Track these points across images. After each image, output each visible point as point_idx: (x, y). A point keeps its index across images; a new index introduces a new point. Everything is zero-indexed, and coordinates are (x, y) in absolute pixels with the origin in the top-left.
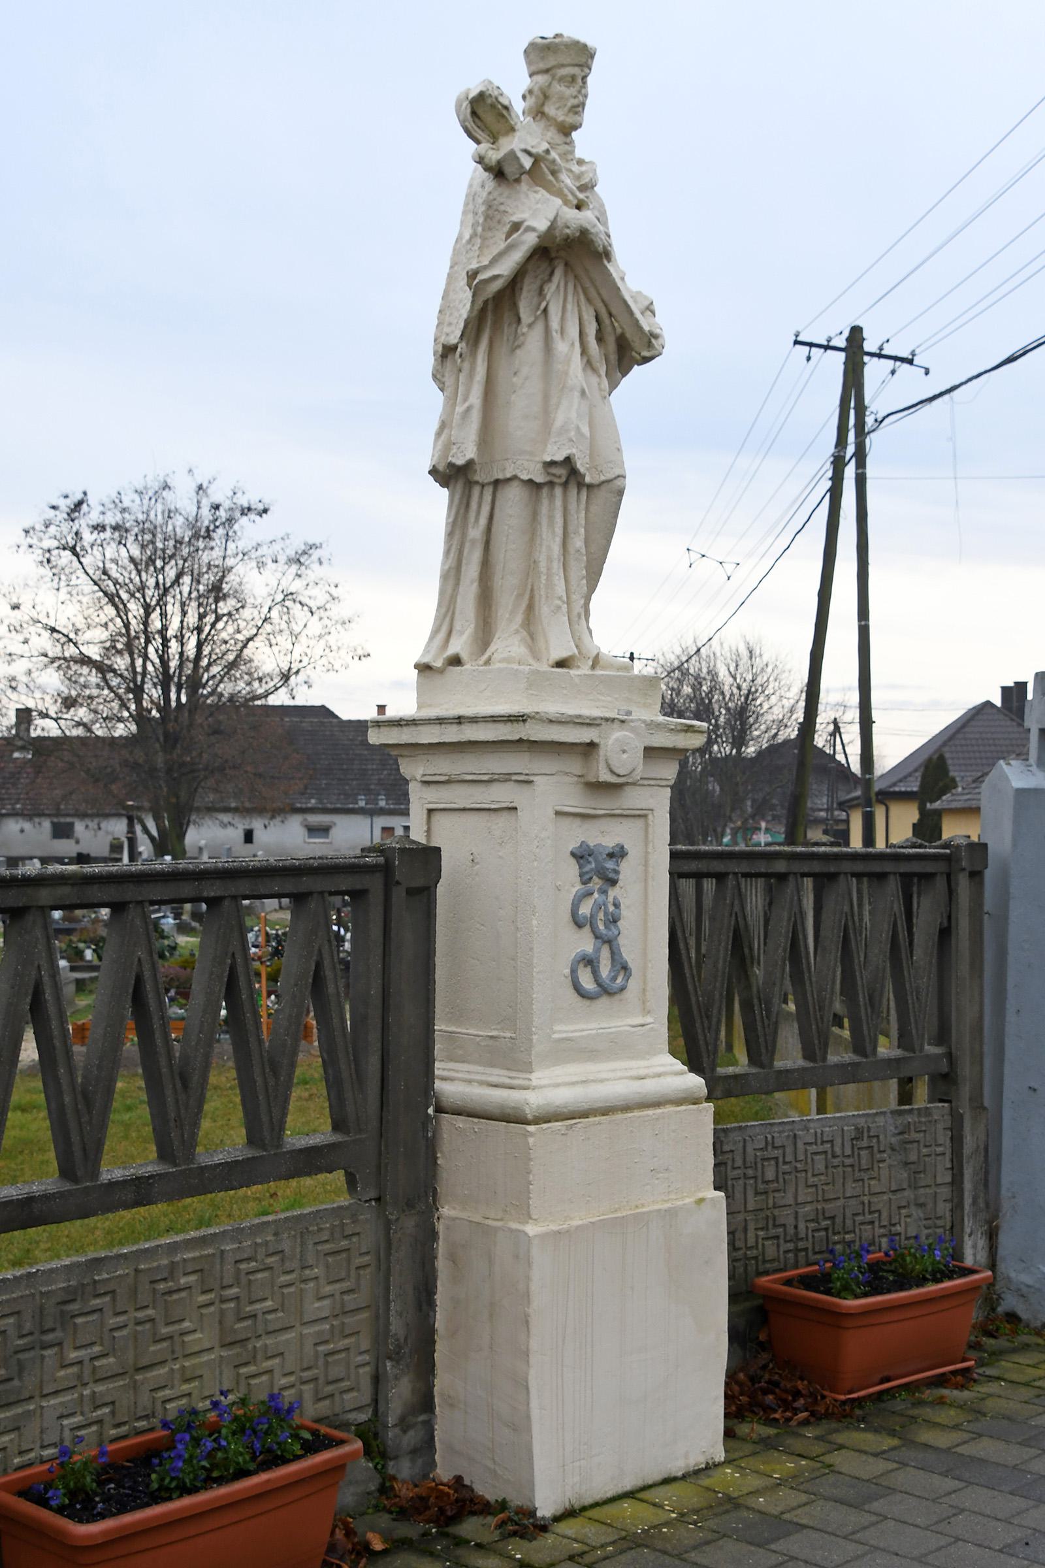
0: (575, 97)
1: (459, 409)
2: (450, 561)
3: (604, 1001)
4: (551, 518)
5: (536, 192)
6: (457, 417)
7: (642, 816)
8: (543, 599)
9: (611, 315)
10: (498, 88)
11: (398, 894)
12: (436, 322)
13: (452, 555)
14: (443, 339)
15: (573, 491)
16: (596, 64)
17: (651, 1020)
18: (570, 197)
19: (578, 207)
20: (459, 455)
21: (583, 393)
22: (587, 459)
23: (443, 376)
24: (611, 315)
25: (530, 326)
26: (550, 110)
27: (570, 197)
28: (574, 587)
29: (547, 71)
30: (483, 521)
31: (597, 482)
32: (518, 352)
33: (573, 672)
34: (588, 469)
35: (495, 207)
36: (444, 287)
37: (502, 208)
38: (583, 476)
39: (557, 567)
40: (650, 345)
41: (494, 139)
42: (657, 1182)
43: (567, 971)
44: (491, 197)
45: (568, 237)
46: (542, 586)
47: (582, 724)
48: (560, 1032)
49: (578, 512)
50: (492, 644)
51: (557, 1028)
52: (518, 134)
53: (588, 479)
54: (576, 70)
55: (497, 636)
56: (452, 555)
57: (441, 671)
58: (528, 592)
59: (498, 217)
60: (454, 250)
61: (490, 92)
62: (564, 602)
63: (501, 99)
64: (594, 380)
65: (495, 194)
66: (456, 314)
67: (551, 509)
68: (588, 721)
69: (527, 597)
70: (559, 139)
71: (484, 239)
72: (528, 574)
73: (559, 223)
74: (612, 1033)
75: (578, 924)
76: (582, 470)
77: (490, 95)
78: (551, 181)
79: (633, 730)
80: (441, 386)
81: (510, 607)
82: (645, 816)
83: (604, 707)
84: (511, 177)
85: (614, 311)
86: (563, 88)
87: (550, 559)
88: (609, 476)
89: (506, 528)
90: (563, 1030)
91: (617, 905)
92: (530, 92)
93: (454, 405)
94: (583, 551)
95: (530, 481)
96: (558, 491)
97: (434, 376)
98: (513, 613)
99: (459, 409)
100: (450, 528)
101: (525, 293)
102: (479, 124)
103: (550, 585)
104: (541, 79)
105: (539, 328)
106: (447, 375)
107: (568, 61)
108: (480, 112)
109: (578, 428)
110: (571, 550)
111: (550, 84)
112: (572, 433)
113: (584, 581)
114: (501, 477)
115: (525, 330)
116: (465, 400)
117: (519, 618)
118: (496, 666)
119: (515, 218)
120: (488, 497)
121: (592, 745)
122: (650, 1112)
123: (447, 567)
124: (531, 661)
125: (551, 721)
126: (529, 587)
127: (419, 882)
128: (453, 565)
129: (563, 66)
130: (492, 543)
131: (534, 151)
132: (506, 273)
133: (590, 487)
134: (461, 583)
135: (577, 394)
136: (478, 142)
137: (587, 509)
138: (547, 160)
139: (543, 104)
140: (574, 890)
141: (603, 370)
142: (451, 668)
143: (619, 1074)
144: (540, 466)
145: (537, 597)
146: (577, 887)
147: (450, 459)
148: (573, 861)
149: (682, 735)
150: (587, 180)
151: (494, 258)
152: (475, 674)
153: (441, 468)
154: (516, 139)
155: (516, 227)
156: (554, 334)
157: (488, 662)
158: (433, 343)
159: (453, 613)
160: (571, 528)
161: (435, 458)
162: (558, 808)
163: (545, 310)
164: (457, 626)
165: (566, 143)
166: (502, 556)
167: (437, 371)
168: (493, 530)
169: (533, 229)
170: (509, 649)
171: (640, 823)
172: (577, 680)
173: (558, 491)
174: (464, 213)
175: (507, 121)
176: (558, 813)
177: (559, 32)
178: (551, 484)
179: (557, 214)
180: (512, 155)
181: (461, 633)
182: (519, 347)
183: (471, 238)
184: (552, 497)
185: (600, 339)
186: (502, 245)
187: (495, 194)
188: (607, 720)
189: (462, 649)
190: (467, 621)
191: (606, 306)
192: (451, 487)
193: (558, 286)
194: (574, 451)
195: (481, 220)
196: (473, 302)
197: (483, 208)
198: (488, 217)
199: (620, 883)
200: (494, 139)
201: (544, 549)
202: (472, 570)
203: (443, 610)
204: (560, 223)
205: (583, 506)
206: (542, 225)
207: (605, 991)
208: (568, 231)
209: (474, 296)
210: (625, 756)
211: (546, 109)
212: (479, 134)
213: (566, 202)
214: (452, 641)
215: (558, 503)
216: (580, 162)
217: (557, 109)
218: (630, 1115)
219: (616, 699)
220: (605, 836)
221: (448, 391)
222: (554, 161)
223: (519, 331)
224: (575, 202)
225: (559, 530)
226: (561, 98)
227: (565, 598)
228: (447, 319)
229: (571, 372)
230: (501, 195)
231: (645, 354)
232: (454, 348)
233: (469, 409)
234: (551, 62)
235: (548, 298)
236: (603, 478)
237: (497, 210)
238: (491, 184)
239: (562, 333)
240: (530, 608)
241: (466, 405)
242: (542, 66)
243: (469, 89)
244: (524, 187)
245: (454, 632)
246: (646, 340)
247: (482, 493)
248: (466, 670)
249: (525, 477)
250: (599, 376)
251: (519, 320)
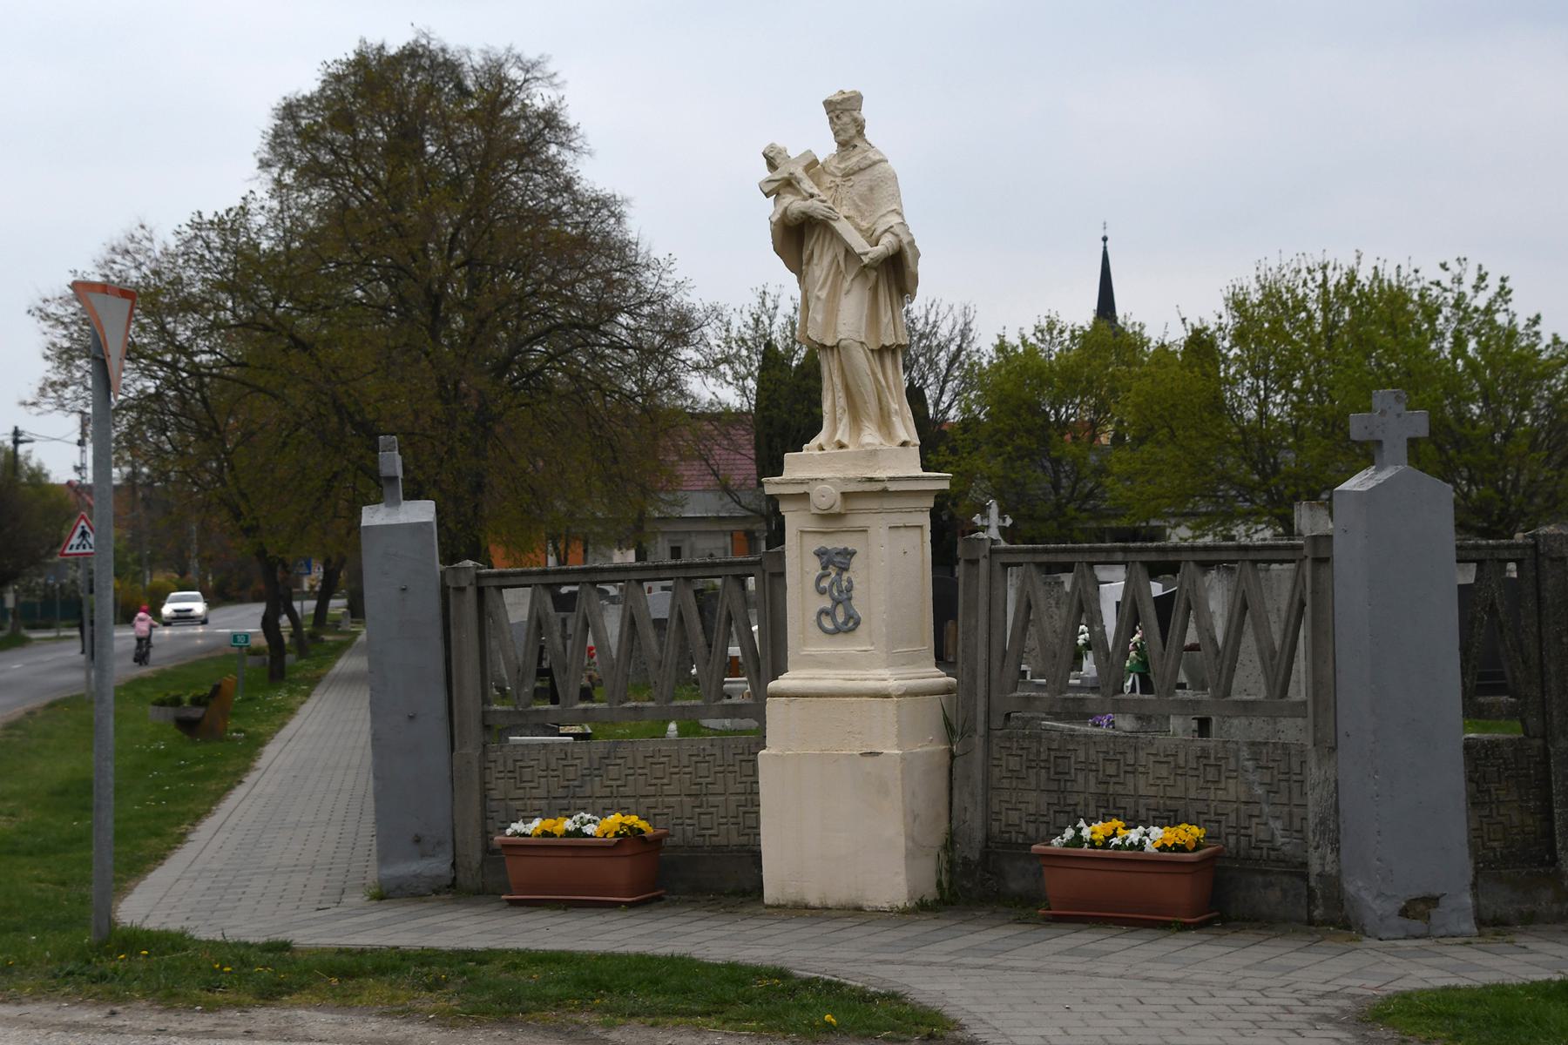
3: (840, 636)
17: (872, 648)
43: (815, 618)
75: (822, 592)
82: (866, 531)
90: (811, 650)
91: (850, 581)
127: (776, 570)
140: (817, 574)
146: (820, 571)
148: (816, 557)
176: (802, 532)
204: (788, 213)
207: (837, 631)
220: (833, 543)
224: (807, 195)
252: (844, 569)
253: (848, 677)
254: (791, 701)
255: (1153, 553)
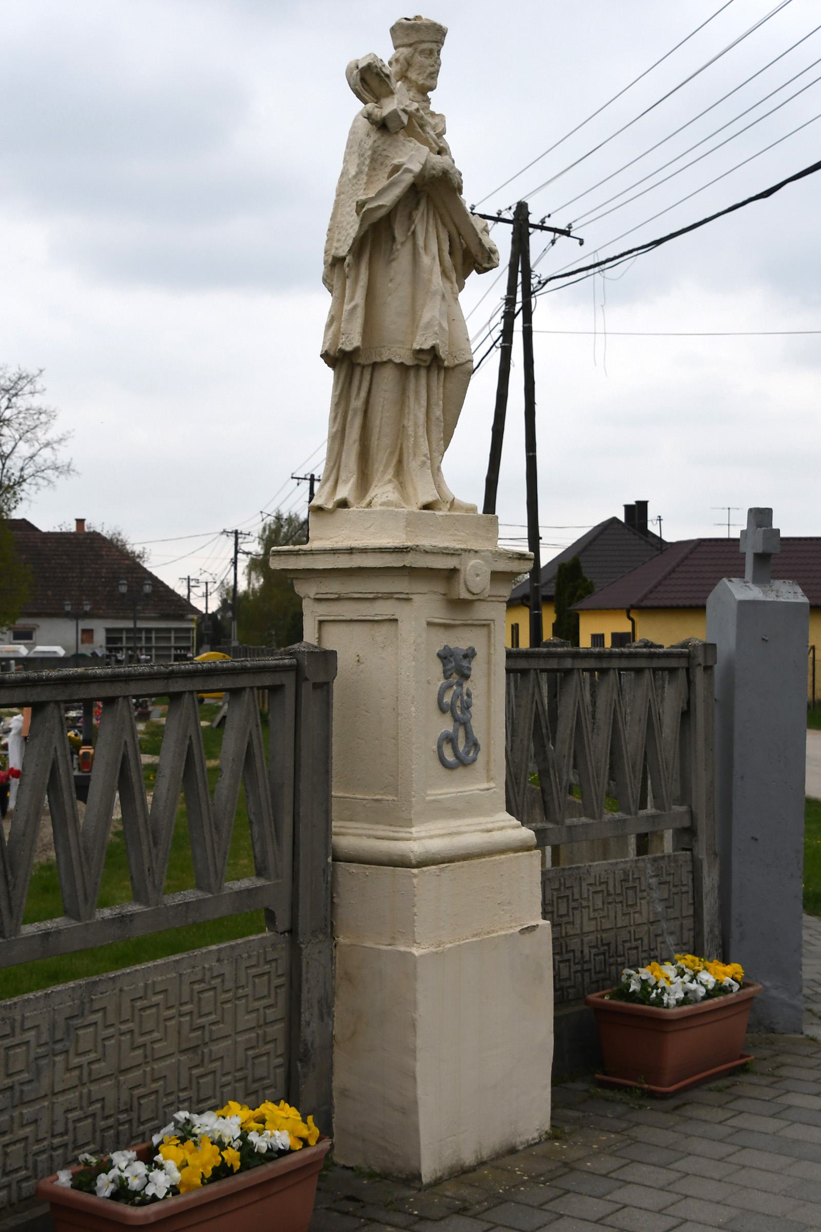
0: (433, 66)
1: (347, 307)
2: (337, 425)
3: (461, 771)
4: (417, 393)
5: (410, 141)
6: (345, 314)
7: (486, 626)
8: (411, 458)
9: (460, 235)
10: (381, 60)
11: (306, 688)
12: (326, 238)
13: (338, 420)
14: (333, 252)
15: (434, 373)
16: (448, 40)
18: (434, 145)
19: (439, 153)
20: (348, 343)
21: (443, 297)
22: (447, 348)
23: (332, 280)
24: (460, 235)
25: (403, 244)
26: (413, 75)
27: (434, 145)
28: (434, 446)
29: (410, 45)
30: (363, 394)
31: (452, 365)
32: (394, 264)
33: (437, 513)
34: (447, 355)
35: (379, 153)
36: (332, 211)
37: (385, 153)
38: (443, 361)
39: (422, 431)
40: (490, 259)
41: (377, 99)
42: (502, 913)
43: (435, 747)
44: (376, 145)
45: (434, 176)
46: (411, 446)
47: (448, 554)
48: (432, 795)
49: (438, 389)
50: (371, 491)
51: (429, 792)
52: (396, 96)
53: (446, 363)
54: (434, 46)
55: (374, 484)
56: (338, 420)
57: (331, 512)
58: (398, 450)
59: (382, 160)
60: (340, 182)
61: (376, 64)
62: (428, 459)
63: (384, 70)
64: (448, 285)
65: (379, 142)
66: (344, 232)
67: (417, 386)
68: (452, 552)
69: (397, 453)
70: (419, 97)
71: (369, 176)
72: (398, 436)
73: (428, 166)
74: (467, 796)
76: (443, 356)
77: (376, 67)
78: (419, 132)
79: (483, 558)
80: (330, 288)
81: (384, 462)
83: (459, 540)
84: (392, 131)
85: (463, 232)
86: (423, 59)
87: (416, 425)
88: (462, 361)
89: (382, 400)
92: (397, 60)
93: (342, 303)
94: (442, 418)
95: (402, 364)
96: (423, 373)
97: (325, 281)
98: (387, 466)
99: (347, 307)
100: (336, 400)
101: (398, 219)
102: (366, 87)
103: (416, 444)
104: (405, 51)
105: (409, 246)
106: (335, 279)
107: (428, 38)
108: (368, 78)
109: (440, 324)
110: (433, 419)
111: (413, 55)
112: (437, 328)
113: (442, 442)
114: (378, 360)
115: (399, 247)
116: (352, 299)
117: (391, 471)
118: (374, 509)
119: (396, 161)
120: (367, 376)
121: (454, 572)
122: (497, 858)
123: (334, 430)
124: (403, 504)
125: (426, 552)
126: (399, 446)
127: (321, 679)
128: (340, 429)
129: (423, 42)
130: (370, 411)
131: (409, 109)
132: (388, 204)
133: (447, 369)
134: (346, 442)
135: (439, 298)
136: (365, 102)
137: (444, 387)
138: (417, 116)
139: (407, 70)
140: (440, 683)
141: (454, 278)
142: (340, 509)
143: (474, 828)
144: (409, 353)
145: (405, 455)
146: (442, 681)
147: (340, 346)
148: (438, 661)
149: (516, 563)
150: (440, 130)
151: (379, 191)
152: (361, 514)
153: (332, 353)
154: (396, 101)
155: (396, 168)
156: (420, 250)
157: (369, 505)
158: (323, 255)
159: (339, 466)
160: (433, 401)
161: (327, 345)
162: (429, 619)
163: (414, 233)
164: (343, 476)
165: (424, 101)
166: (378, 422)
167: (327, 276)
168: (371, 401)
169: (408, 171)
170: (385, 495)
171: (484, 631)
172: (440, 520)
173: (423, 373)
174: (348, 153)
175: (388, 86)
176: (429, 624)
177: (418, 14)
178: (417, 367)
179: (426, 160)
180: (394, 113)
181: (346, 482)
182: (394, 260)
183: (357, 174)
184: (417, 377)
185: (451, 253)
186: (385, 183)
187: (379, 142)
188: (465, 550)
189: (349, 495)
190: (351, 472)
191: (457, 229)
192: (337, 368)
193: (423, 214)
194: (438, 341)
195: (367, 162)
196: (361, 225)
197: (369, 153)
198: (373, 160)
199: (471, 678)
200: (377, 99)
201: (412, 417)
202: (354, 433)
203: (332, 464)
205: (441, 384)
206: (416, 167)
207: (463, 762)
208: (434, 172)
209: (362, 221)
210: (478, 579)
211: (409, 74)
212: (367, 96)
213: (431, 149)
214: (339, 488)
215: (423, 381)
216: (433, 114)
217: (418, 74)
218: (484, 860)
219: (467, 534)
220: (461, 641)
221: (337, 292)
222: (422, 117)
223: (394, 247)
224: (437, 149)
225: (424, 403)
226: (421, 66)
227: (429, 456)
228: (336, 236)
229: (434, 280)
230: (384, 143)
231: (486, 265)
232: (344, 259)
233: (355, 307)
234: (414, 38)
235: (416, 222)
236: (457, 362)
237: (380, 155)
238: (375, 136)
239: (425, 250)
240: (400, 462)
241: (353, 303)
242: (406, 41)
243: (358, 60)
244: (401, 137)
245: (340, 481)
246: (486, 255)
247: (362, 373)
248: (354, 511)
249: (398, 361)
250: (452, 282)
251: (394, 239)
252: (466, 677)
253: (483, 827)
254: (442, 870)
255: (593, 660)
